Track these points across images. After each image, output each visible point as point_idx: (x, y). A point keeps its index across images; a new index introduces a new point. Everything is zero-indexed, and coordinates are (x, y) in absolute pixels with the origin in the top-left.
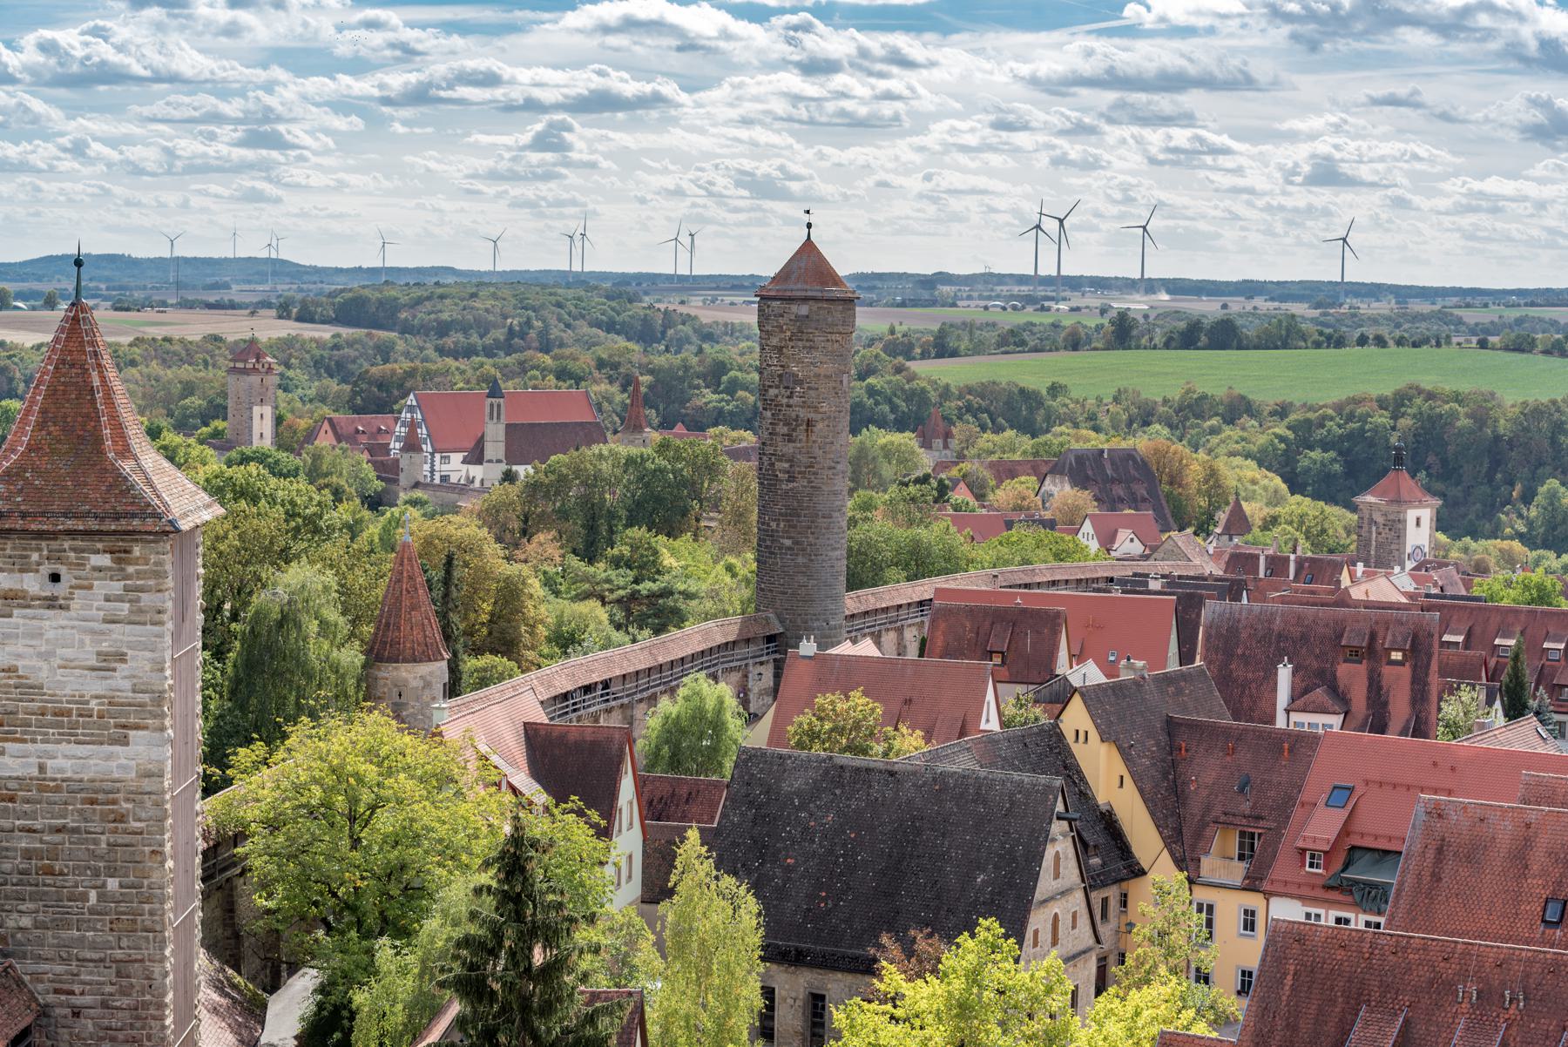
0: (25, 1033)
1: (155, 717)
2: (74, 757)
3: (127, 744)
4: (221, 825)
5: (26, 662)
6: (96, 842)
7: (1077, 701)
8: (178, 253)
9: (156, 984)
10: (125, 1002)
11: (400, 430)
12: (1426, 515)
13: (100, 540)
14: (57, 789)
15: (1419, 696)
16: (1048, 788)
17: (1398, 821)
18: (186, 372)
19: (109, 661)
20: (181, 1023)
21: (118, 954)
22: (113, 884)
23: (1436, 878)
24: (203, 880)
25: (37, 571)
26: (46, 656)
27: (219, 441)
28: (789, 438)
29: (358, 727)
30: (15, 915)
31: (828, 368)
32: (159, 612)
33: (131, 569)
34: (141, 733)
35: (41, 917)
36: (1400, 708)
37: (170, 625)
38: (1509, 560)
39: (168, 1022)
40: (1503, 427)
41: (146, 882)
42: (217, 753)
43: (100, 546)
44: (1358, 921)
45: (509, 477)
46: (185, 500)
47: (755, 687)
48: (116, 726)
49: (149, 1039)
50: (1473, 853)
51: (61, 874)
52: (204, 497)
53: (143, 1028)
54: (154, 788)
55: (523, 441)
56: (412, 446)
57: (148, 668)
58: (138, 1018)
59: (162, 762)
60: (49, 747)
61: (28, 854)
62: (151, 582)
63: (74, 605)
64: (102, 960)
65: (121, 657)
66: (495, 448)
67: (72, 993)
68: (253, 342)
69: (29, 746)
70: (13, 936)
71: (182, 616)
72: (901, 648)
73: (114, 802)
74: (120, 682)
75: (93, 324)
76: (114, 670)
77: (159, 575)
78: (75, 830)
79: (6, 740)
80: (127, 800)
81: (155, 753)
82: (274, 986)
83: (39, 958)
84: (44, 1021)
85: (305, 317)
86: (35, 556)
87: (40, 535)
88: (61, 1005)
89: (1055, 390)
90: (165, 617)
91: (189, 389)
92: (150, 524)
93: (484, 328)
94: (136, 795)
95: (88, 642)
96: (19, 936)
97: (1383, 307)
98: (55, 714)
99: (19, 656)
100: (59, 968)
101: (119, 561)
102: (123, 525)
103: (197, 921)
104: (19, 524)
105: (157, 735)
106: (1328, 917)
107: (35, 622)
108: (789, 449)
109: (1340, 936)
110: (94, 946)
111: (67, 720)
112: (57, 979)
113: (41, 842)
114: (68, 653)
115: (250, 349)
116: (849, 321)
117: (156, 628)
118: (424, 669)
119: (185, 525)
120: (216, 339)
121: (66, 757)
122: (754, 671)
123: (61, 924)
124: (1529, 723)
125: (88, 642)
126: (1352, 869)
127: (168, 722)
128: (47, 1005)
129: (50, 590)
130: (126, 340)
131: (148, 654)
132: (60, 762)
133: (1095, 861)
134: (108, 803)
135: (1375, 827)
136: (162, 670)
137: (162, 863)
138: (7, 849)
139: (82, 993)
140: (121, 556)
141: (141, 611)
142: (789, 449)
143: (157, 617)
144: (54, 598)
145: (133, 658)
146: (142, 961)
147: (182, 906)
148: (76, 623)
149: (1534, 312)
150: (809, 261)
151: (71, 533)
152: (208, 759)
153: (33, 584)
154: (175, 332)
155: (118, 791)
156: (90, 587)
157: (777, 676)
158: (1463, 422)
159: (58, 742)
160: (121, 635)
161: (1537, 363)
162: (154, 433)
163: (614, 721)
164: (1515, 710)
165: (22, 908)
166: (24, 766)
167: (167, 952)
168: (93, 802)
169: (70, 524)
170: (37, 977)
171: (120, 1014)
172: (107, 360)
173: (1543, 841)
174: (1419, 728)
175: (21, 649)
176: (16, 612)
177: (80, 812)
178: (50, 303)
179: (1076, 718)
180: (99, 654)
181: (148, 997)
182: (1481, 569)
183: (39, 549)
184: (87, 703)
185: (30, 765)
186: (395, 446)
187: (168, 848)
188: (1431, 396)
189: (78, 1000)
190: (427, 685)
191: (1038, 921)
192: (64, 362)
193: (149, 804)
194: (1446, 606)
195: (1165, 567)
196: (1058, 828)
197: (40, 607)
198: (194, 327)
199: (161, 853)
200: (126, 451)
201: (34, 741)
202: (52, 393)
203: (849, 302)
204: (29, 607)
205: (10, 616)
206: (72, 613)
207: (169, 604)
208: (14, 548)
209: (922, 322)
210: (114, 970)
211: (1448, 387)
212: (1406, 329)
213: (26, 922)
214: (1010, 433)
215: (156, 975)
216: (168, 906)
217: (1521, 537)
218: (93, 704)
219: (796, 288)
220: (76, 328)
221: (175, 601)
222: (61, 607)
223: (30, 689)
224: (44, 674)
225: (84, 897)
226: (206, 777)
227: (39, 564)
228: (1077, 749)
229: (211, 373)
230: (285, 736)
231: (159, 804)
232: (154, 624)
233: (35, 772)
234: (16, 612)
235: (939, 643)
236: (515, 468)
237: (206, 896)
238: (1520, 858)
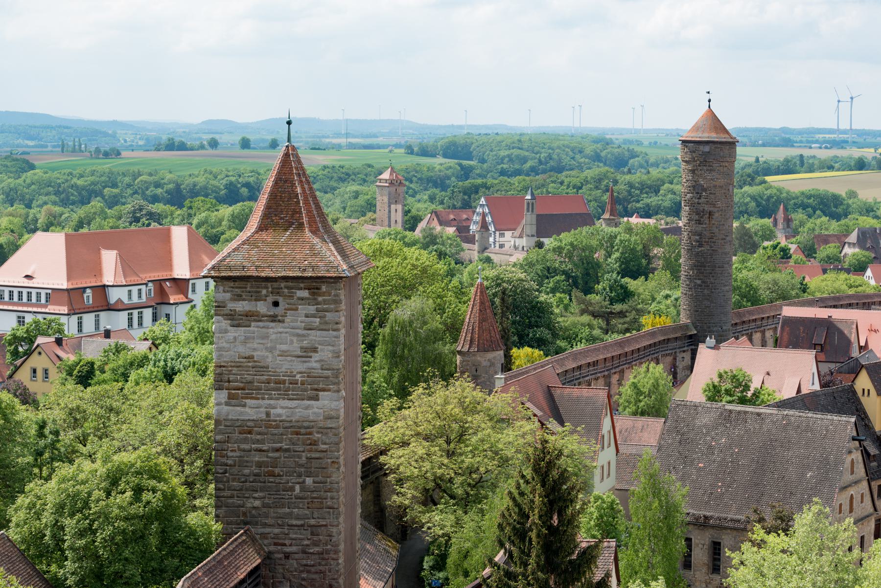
0: (257, 568)
1: (334, 384)
2: (287, 408)
3: (318, 400)
5: (259, 353)
6: (300, 457)
9: (334, 539)
10: (316, 549)
11: (476, 218)
13: (302, 282)
14: (277, 427)
19: (309, 351)
21: (312, 522)
22: (309, 481)
24: (362, 478)
25: (265, 300)
26: (271, 350)
29: (452, 389)
30: (252, 500)
32: (337, 323)
33: (320, 299)
34: (326, 393)
35: (266, 501)
37: (343, 331)
39: (340, 561)
41: (328, 480)
43: (302, 285)
45: (540, 245)
48: (312, 390)
49: (330, 571)
51: (279, 475)
53: (326, 565)
54: (333, 426)
56: (484, 226)
57: (330, 355)
58: (323, 559)
59: (338, 410)
60: (272, 402)
61: (259, 465)
62: (332, 306)
63: (287, 319)
64: (302, 525)
65: (315, 350)
67: (285, 545)
69: (260, 401)
70: (250, 512)
71: (351, 326)
73: (310, 434)
74: (314, 363)
76: (311, 357)
77: (337, 302)
78: (287, 450)
79: (247, 398)
80: (318, 432)
81: (334, 405)
83: (265, 525)
84: (268, 562)
86: (264, 292)
87: (267, 279)
88: (278, 552)
90: (340, 326)
93: (525, 160)
94: (324, 430)
95: (295, 341)
96: (254, 512)
98: (276, 383)
99: (255, 350)
100: (277, 531)
101: (313, 294)
103: (359, 502)
104: (255, 274)
105: (336, 394)
107: (264, 330)
111: (284, 386)
112: (276, 536)
113: (267, 457)
114: (284, 347)
117: (335, 333)
118: (490, 355)
121: (282, 408)
125: (295, 341)
127: (342, 386)
128: (270, 552)
129: (273, 311)
131: (330, 348)
132: (279, 411)
134: (306, 434)
136: (338, 357)
137: (338, 469)
138: (247, 462)
139: (291, 545)
141: (326, 323)
143: (335, 327)
144: (275, 316)
145: (322, 350)
146: (326, 526)
148: (288, 330)
155: (313, 427)
156: (297, 309)
159: (278, 399)
160: (315, 336)
165: (256, 495)
166: (257, 413)
167: (341, 520)
168: (297, 434)
169: (283, 274)
170: (264, 536)
171: (313, 557)
175: (256, 346)
176: (253, 324)
177: (290, 440)
180: (301, 348)
181: (329, 547)
183: (267, 288)
184: (295, 376)
185: (261, 412)
186: (473, 228)
187: (341, 460)
190: (492, 364)
192: (281, 179)
193: (330, 435)
197: (267, 321)
199: (338, 463)
201: (263, 399)
204: (260, 321)
205: (249, 326)
206: (286, 324)
207: (343, 319)
208: (251, 287)
210: (309, 532)
213: (257, 503)
215: (334, 534)
216: (341, 493)
218: (298, 377)
221: (346, 317)
222: (279, 321)
224: (270, 360)
225: (292, 489)
227: (266, 296)
230: (410, 394)
232: (334, 330)
233: (264, 416)
234: (253, 324)
236: (542, 240)
237: (363, 487)
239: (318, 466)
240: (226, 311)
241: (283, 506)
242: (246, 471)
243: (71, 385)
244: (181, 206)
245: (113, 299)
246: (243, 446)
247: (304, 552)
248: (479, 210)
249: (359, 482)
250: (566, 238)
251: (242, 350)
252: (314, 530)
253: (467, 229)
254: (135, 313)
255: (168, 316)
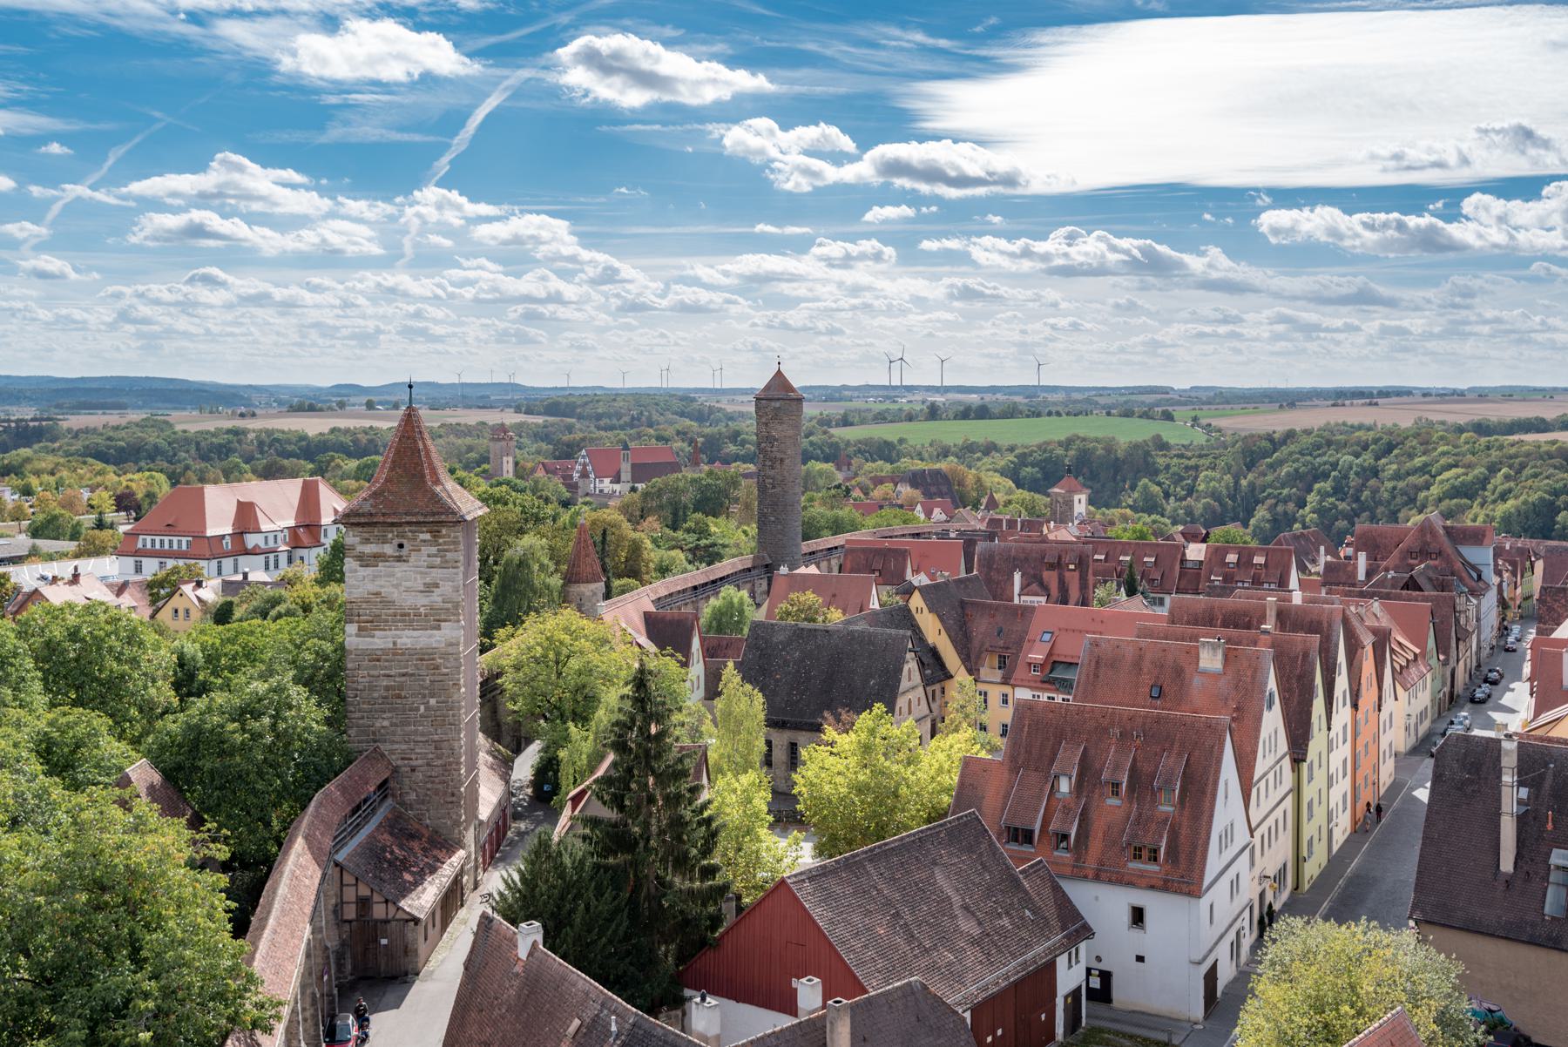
0: (385, 782)
4: (491, 670)
7: (917, 593)
8: (464, 380)
11: (578, 467)
12: (1083, 497)
15: (1084, 586)
16: (904, 637)
17: (1075, 648)
18: (468, 440)
19: (430, 587)
20: (469, 772)
21: (436, 737)
22: (433, 701)
23: (1096, 676)
26: (396, 586)
27: (486, 475)
28: (772, 468)
31: (790, 433)
36: (1074, 593)
38: (1125, 519)
40: (1120, 454)
42: (488, 631)
44: (1059, 698)
45: (633, 490)
46: (470, 506)
47: (758, 590)
50: (1114, 664)
52: (479, 503)
55: (640, 472)
56: (584, 475)
61: (387, 688)
63: (412, 559)
65: (437, 586)
66: (626, 475)
68: (503, 425)
71: (468, 563)
72: (830, 570)
74: (436, 598)
75: (419, 417)
77: (456, 543)
81: (455, 633)
82: (518, 751)
85: (529, 412)
87: (393, 524)
89: (901, 441)
91: (470, 449)
92: (451, 518)
93: (619, 416)
94: (445, 656)
97: (1060, 397)
100: (404, 747)
102: (437, 518)
106: (1044, 697)
108: (772, 473)
109: (1050, 707)
110: (423, 734)
111: (408, 618)
114: (408, 584)
115: (502, 428)
116: (800, 410)
118: (593, 586)
119: (469, 518)
120: (484, 423)
122: (757, 582)
123: (405, 723)
124: (1139, 598)
126: (1053, 672)
130: (436, 425)
132: (405, 640)
133: (928, 672)
135: (1065, 651)
140: (436, 534)
142: (772, 473)
147: (470, 712)
149: (1134, 397)
150: (779, 379)
151: (409, 523)
152: (483, 635)
153: (389, 549)
154: (462, 421)
157: (769, 585)
158: (1100, 452)
160: (436, 574)
161: (1136, 421)
162: (452, 471)
163: (689, 610)
164: (1131, 592)
169: (408, 519)
170: (392, 752)
172: (426, 436)
173: (1148, 656)
174: (1084, 602)
178: (396, 406)
179: (916, 601)
182: (1112, 523)
186: (576, 475)
188: (1084, 439)
189: (414, 763)
190: (595, 594)
191: (901, 702)
194: (1095, 541)
195: (957, 525)
196: (910, 656)
198: (471, 418)
200: (437, 482)
202: (398, 452)
203: (800, 400)
209: (835, 410)
211: (1092, 435)
212: (1071, 408)
213: (386, 723)
214: (880, 463)
217: (1130, 507)
219: (776, 394)
220: (410, 419)
223: (387, 603)
225: (418, 709)
226: (482, 644)
228: (917, 617)
229: (481, 441)
231: (457, 660)
235: (848, 566)
238: (1137, 664)
239: (442, 687)
240: (355, 553)
241: (409, 724)
242: (376, 695)
243: (210, 624)
244: (312, 461)
245: (250, 546)
246: (375, 673)
247: (428, 765)
248: (581, 460)
249: (478, 700)
250: (658, 481)
251: (372, 587)
252: (437, 745)
253: (571, 477)
254: (272, 556)
255: (302, 558)
